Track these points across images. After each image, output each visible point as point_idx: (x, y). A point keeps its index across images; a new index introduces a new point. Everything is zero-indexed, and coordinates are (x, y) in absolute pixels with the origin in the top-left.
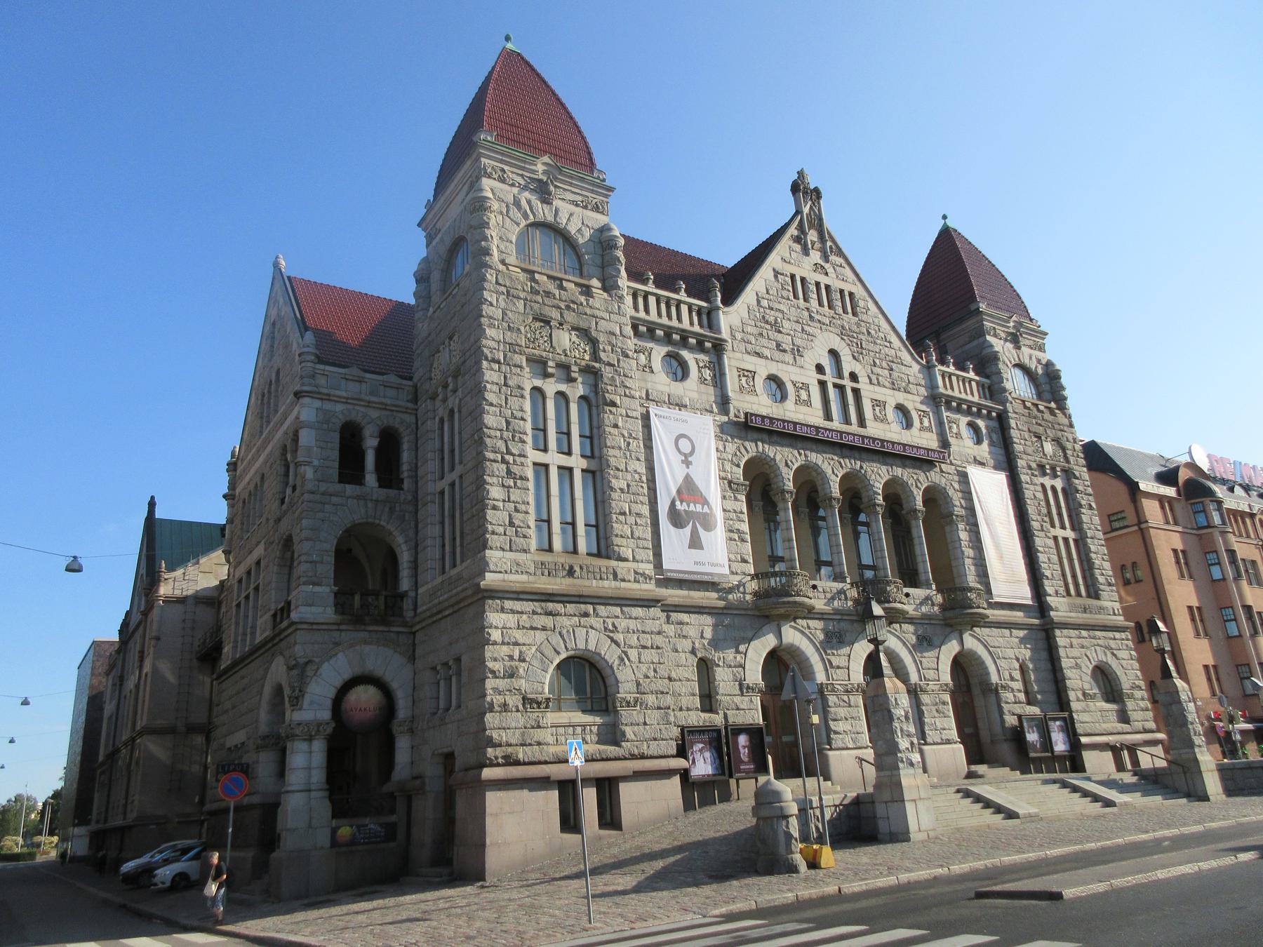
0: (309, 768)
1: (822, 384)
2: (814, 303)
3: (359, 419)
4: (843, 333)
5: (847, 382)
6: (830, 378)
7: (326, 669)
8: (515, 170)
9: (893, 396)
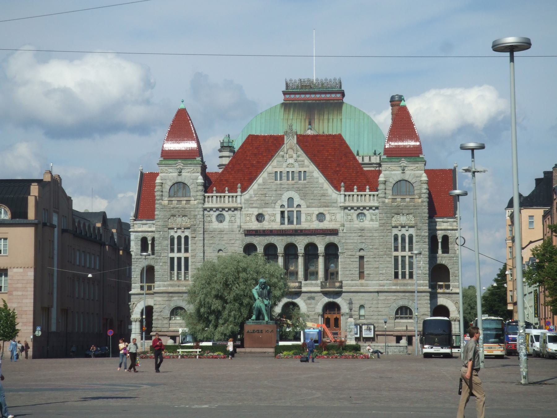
0: (136, 329)
1: (282, 213)
2: (284, 181)
3: (145, 236)
4: (298, 190)
5: (295, 209)
6: (286, 209)
7: (138, 305)
8: (169, 168)
9: (318, 210)
